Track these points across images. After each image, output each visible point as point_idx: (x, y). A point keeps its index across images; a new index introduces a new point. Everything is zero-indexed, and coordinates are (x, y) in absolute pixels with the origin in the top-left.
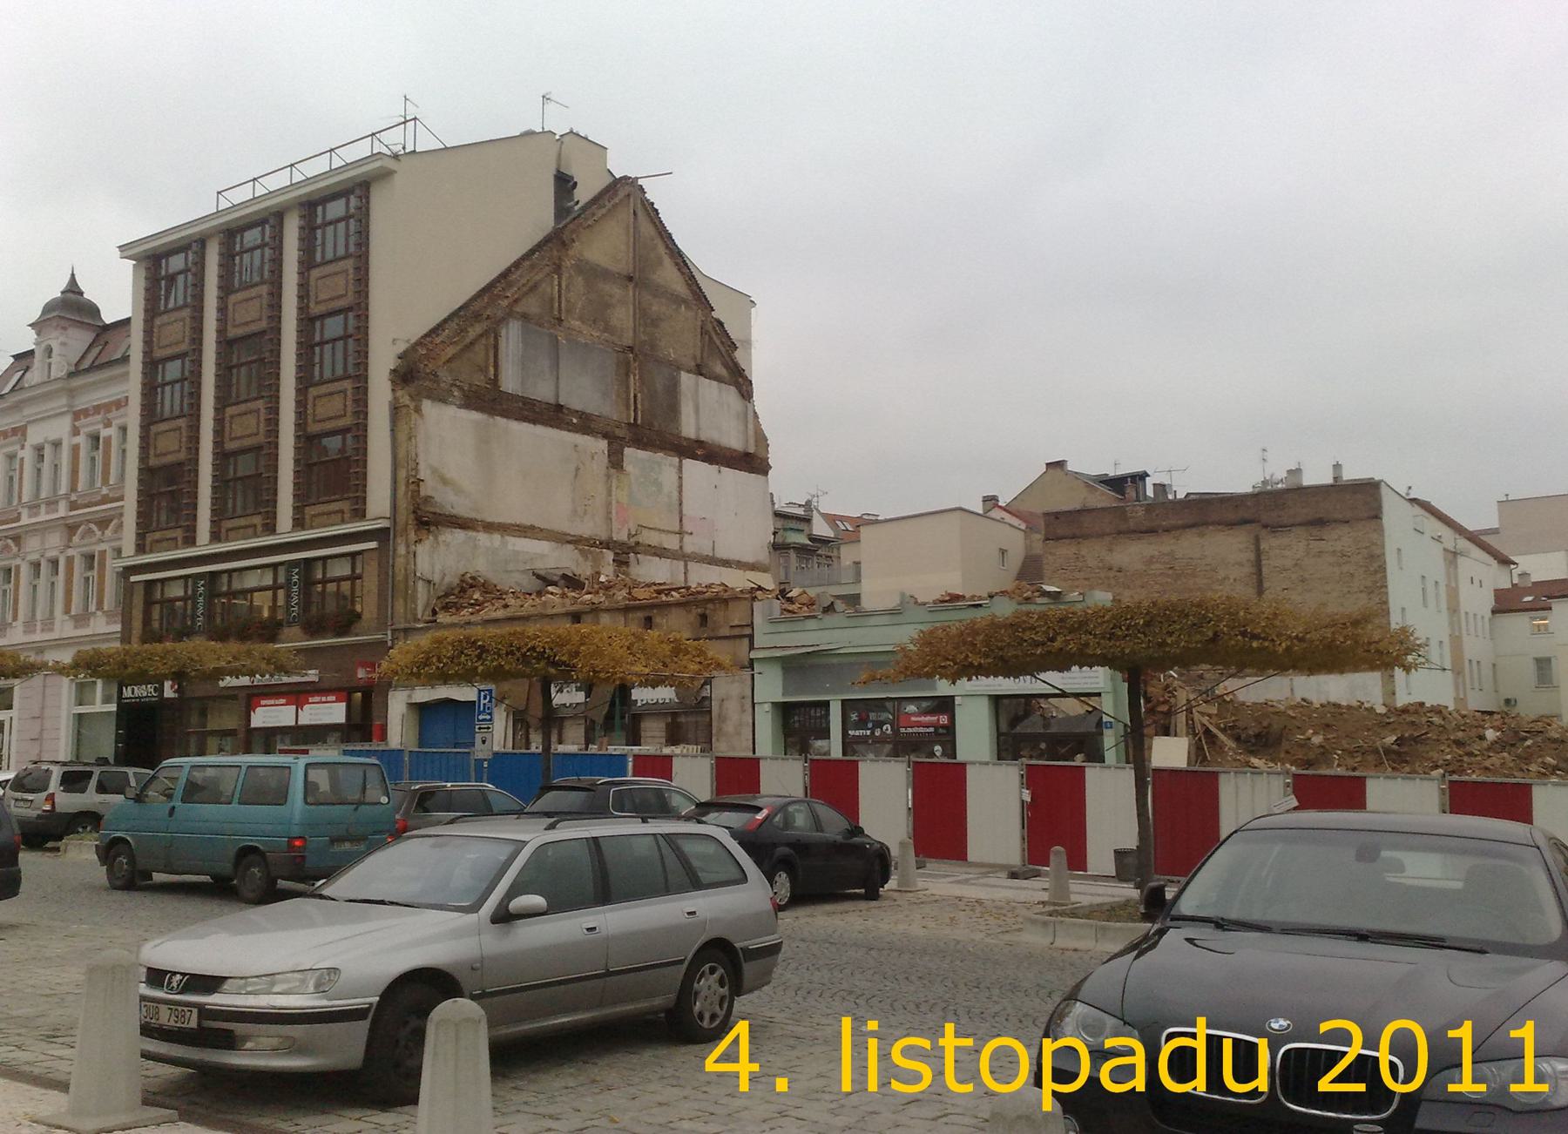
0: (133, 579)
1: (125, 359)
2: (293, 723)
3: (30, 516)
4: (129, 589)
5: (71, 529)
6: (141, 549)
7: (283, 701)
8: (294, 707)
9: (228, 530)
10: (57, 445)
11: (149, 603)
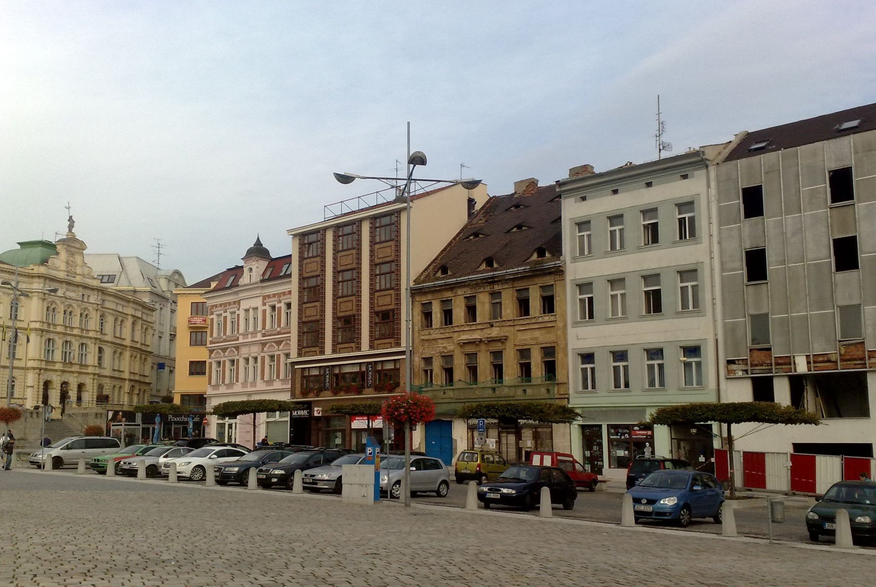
0: (296, 367)
1: (290, 276)
3: (243, 339)
4: (294, 372)
6: (300, 355)
9: (340, 349)
10: (255, 309)
11: (303, 377)
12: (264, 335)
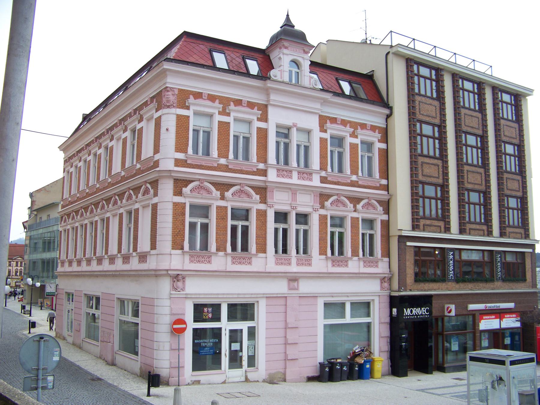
2: (498, 327)
5: (323, 197)
7: (493, 317)
8: (498, 320)
9: (470, 229)
12: (323, 180)
